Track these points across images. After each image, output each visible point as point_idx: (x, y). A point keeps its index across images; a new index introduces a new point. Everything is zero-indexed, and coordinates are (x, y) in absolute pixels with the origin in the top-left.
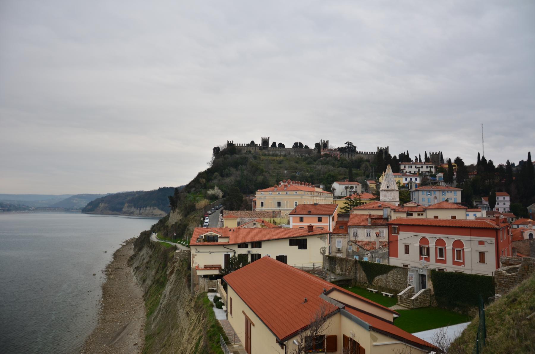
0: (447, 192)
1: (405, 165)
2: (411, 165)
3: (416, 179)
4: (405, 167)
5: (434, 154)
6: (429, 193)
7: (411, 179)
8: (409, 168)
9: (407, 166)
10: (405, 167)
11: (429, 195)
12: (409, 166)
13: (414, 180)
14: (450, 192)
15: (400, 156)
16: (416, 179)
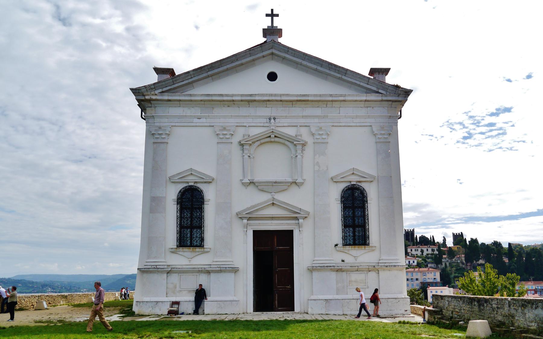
0: (428, 273)
1: (411, 249)
2: (417, 248)
3: (414, 262)
4: (411, 250)
5: (458, 234)
6: (424, 274)
7: (409, 262)
8: (415, 251)
9: (413, 250)
10: (411, 250)
11: (425, 275)
12: (415, 249)
13: (411, 262)
14: (430, 273)
15: (420, 238)
16: (414, 262)
